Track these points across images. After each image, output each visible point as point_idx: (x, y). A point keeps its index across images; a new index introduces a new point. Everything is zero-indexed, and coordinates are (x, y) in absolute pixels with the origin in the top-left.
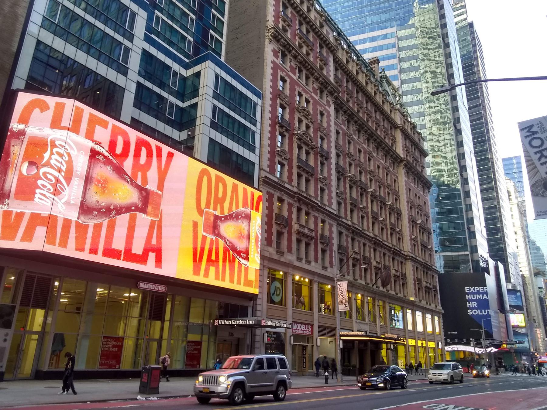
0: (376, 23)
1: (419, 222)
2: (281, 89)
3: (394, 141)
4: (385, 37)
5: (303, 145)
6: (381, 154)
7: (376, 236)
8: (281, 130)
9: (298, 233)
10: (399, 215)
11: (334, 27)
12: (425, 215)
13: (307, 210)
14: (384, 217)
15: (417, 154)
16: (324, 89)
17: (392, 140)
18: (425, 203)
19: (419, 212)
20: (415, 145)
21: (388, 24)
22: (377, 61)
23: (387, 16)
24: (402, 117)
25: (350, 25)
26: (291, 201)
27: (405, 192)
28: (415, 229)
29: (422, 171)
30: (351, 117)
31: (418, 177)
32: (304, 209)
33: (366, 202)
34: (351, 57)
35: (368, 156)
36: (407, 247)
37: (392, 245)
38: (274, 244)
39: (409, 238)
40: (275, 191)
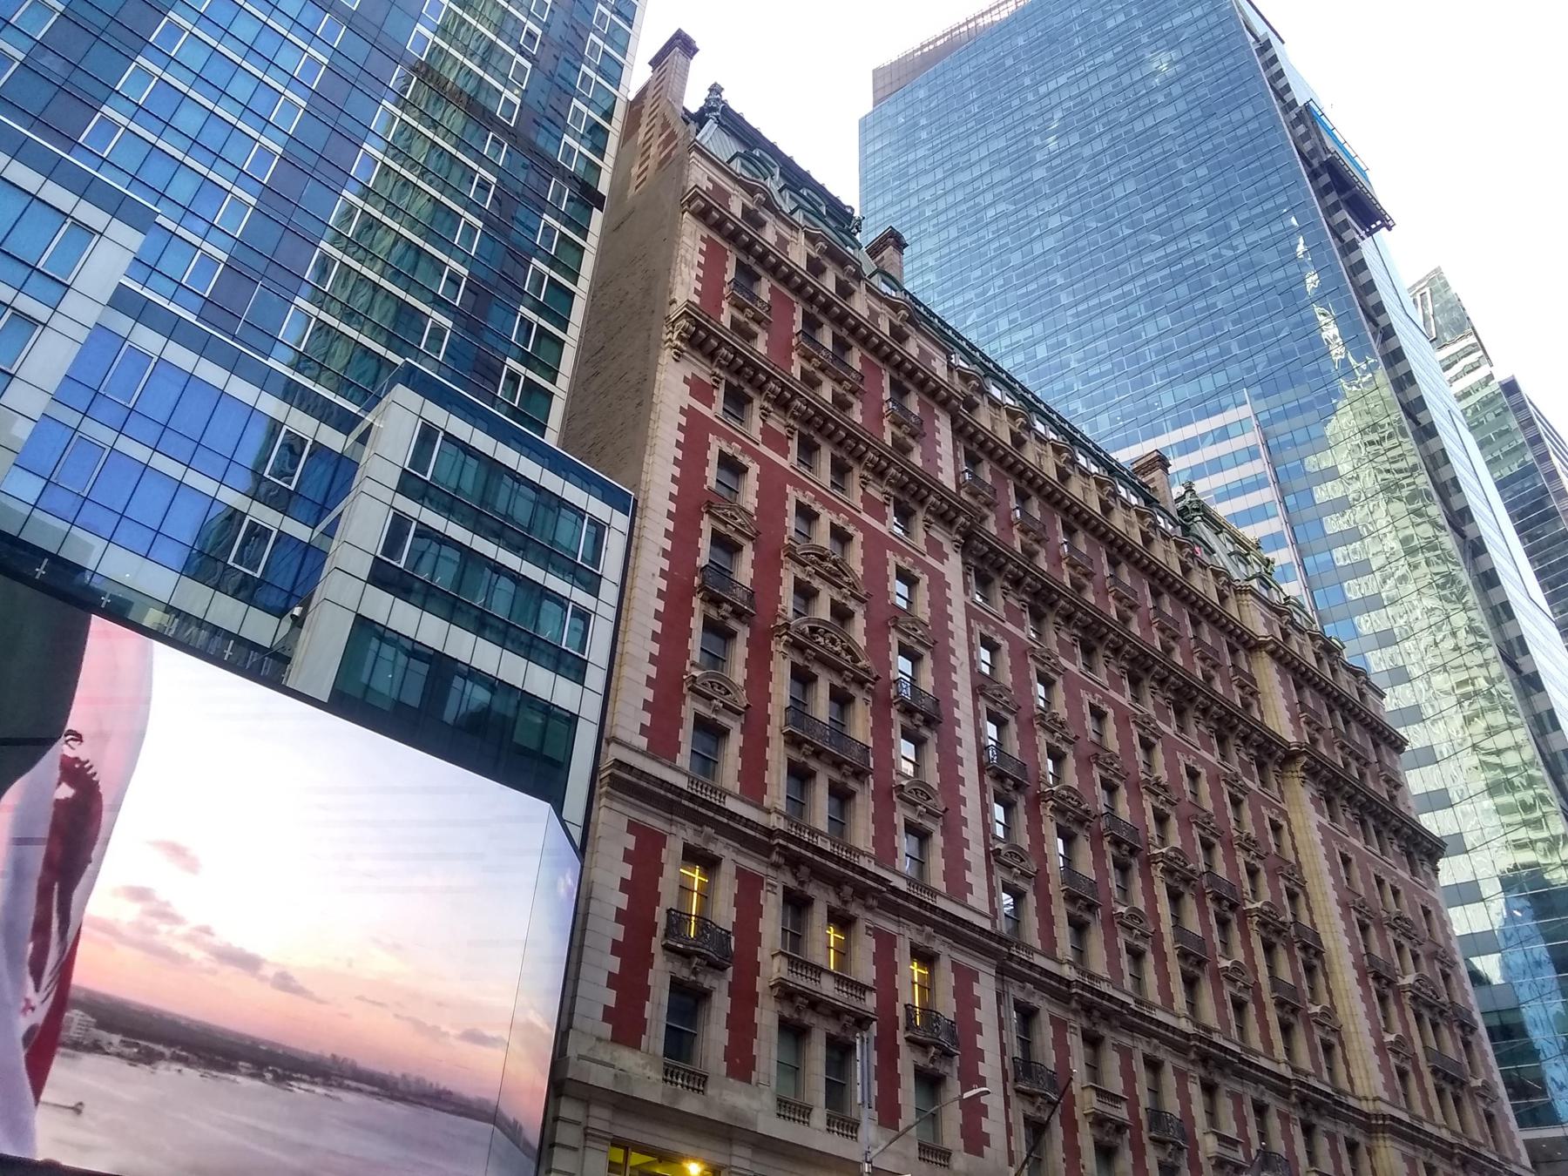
0: (1190, 403)
1: (1409, 979)
2: (903, 604)
3: (1250, 688)
4: (1223, 434)
5: (815, 669)
6: (1195, 730)
7: (1208, 1030)
8: (908, 723)
9: (786, 993)
10: (1313, 953)
11: (947, 339)
12: (1433, 956)
13: (835, 903)
14: (1239, 955)
15: (1357, 736)
16: (913, 505)
17: (1242, 687)
18: (1427, 913)
19: (1404, 941)
20: (1343, 706)
21: (1225, 400)
22: (1160, 461)
23: (1221, 379)
24: (1272, 616)
25: (1113, 421)
26: (752, 865)
27: (1325, 865)
28: (1393, 1009)
29: (1392, 798)
30: (1042, 601)
31: (1376, 817)
32: (822, 900)
33: (1240, 950)
34: (1115, 494)
35: (1136, 731)
36: (1367, 1079)
37: (1295, 1070)
38: (655, 1038)
39: (1371, 1042)
40: (671, 822)
